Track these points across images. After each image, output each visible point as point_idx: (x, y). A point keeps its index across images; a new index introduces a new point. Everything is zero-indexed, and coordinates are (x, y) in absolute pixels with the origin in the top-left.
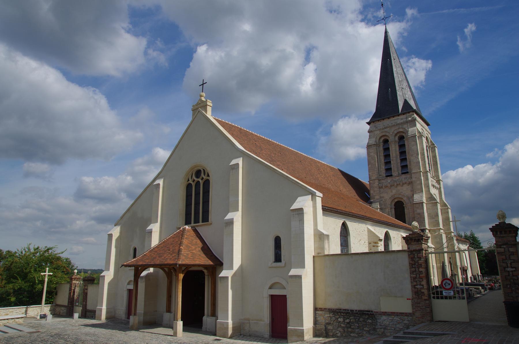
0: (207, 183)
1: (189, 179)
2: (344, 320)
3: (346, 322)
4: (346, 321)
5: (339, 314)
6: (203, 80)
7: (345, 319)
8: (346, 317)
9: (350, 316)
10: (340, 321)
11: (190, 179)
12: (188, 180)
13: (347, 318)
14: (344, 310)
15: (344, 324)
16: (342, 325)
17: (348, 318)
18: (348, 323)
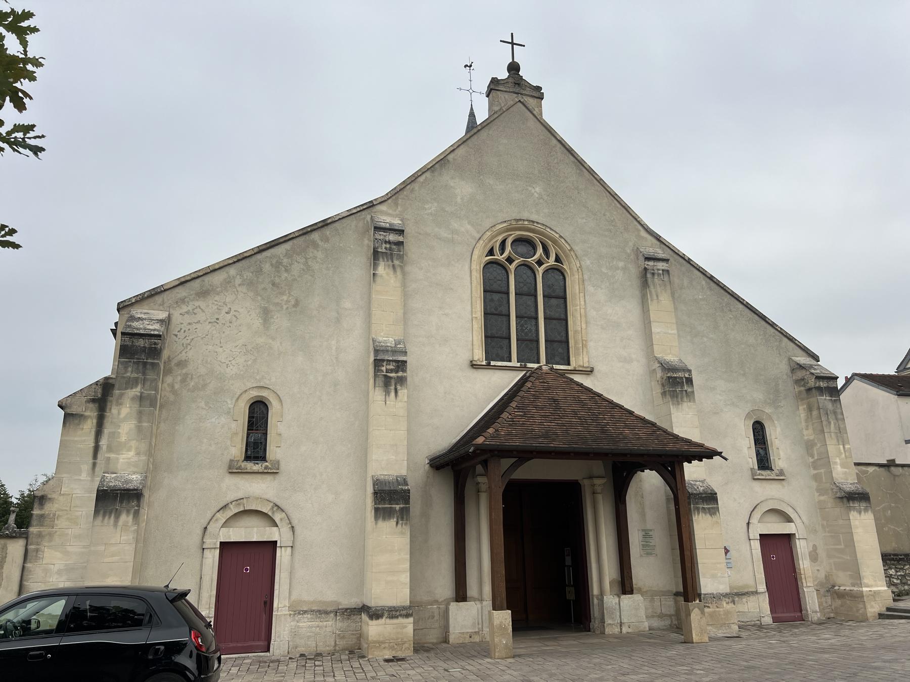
0: (557, 272)
1: (493, 247)
2: (897, 572)
3: (901, 575)
4: (900, 574)
5: (888, 562)
6: (512, 34)
7: (898, 570)
8: (899, 567)
9: (905, 565)
10: (892, 575)
11: (497, 250)
12: (491, 252)
13: (900, 569)
14: (895, 555)
15: (898, 579)
16: (895, 581)
17: (902, 569)
18: (904, 576)
